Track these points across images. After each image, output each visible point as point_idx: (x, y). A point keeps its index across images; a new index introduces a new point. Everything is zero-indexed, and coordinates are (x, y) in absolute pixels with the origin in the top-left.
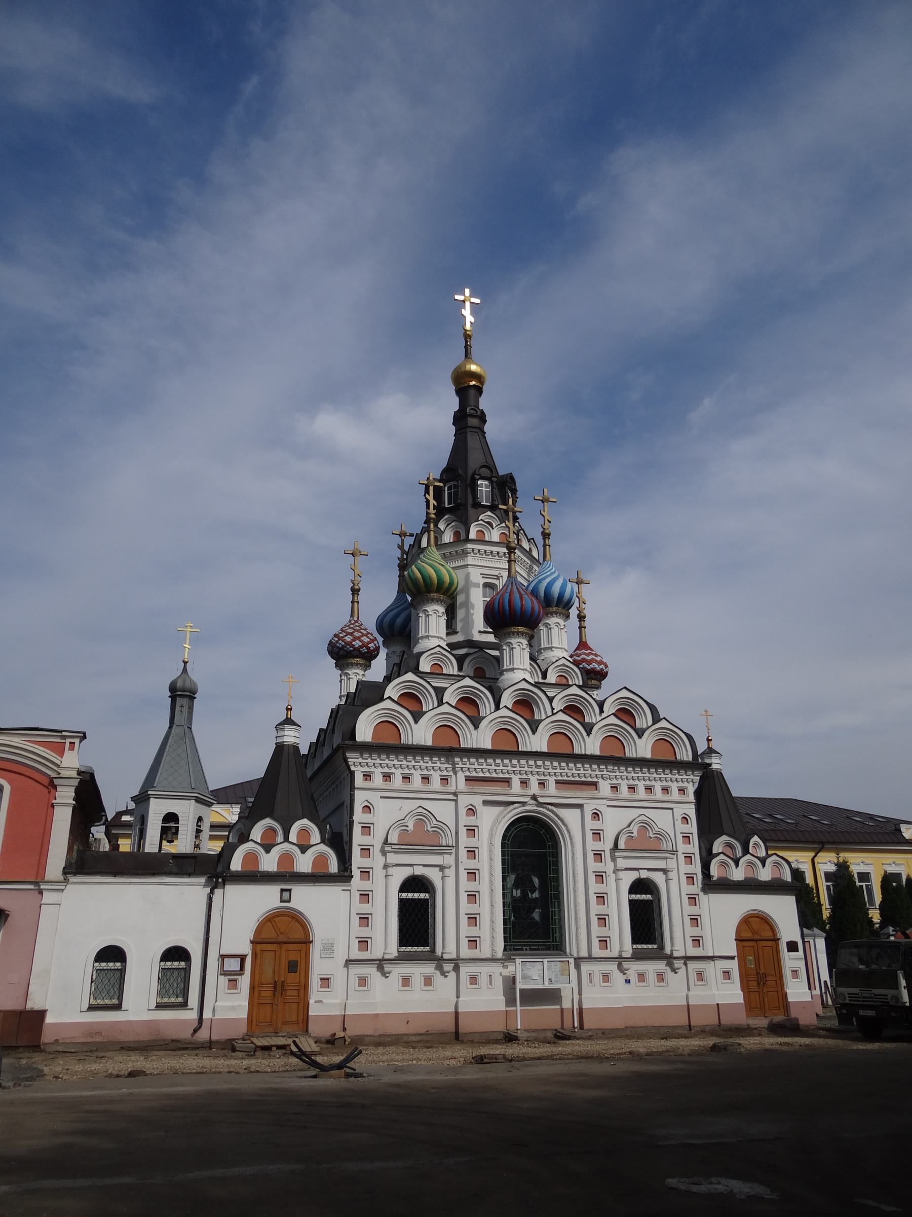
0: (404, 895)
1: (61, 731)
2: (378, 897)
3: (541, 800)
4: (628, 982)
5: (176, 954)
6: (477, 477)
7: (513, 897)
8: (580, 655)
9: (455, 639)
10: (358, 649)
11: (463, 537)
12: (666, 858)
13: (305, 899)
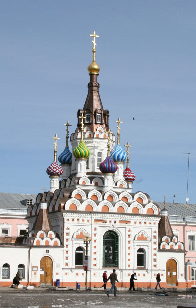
0: (77, 252)
2: (70, 252)
3: (115, 226)
5: (21, 266)
10: (57, 173)
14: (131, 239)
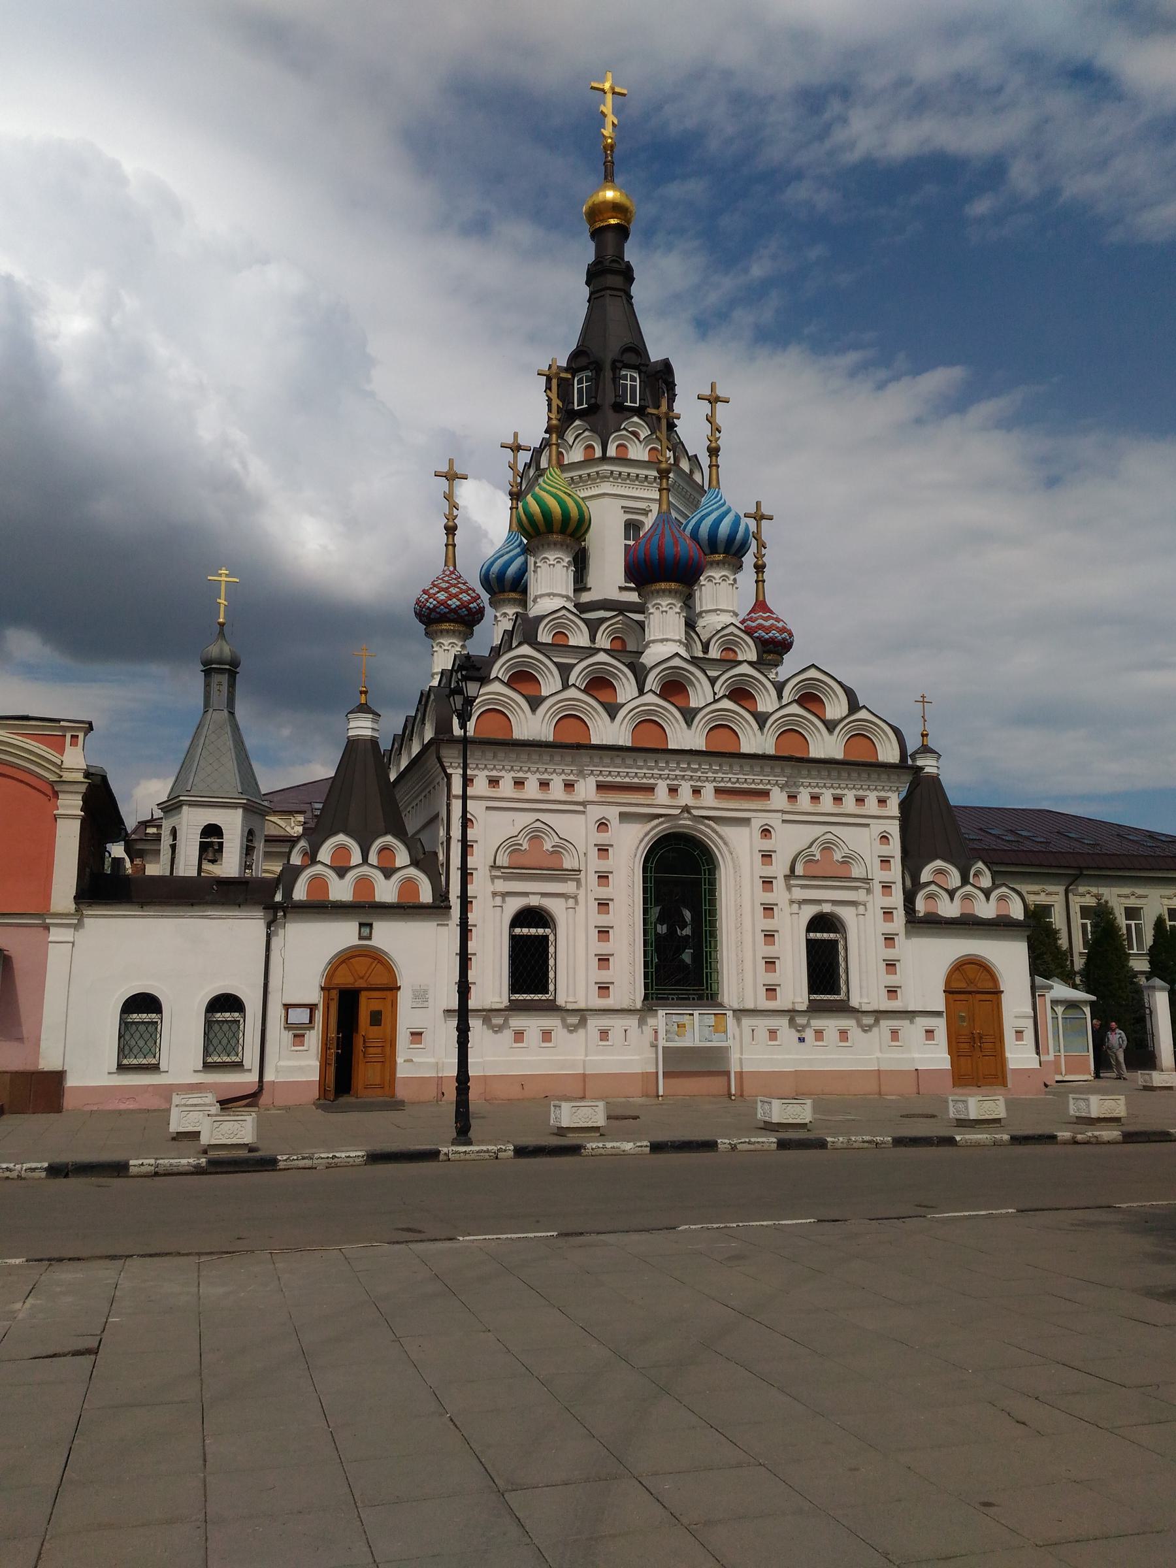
1: (59, 721)
3: (695, 812)
4: (802, 1040)
5: (225, 1004)
6: (619, 365)
7: (657, 934)
8: (757, 619)
9: (586, 597)
10: (454, 611)
11: (598, 453)
12: (857, 888)
13: (389, 936)
14: (779, 868)
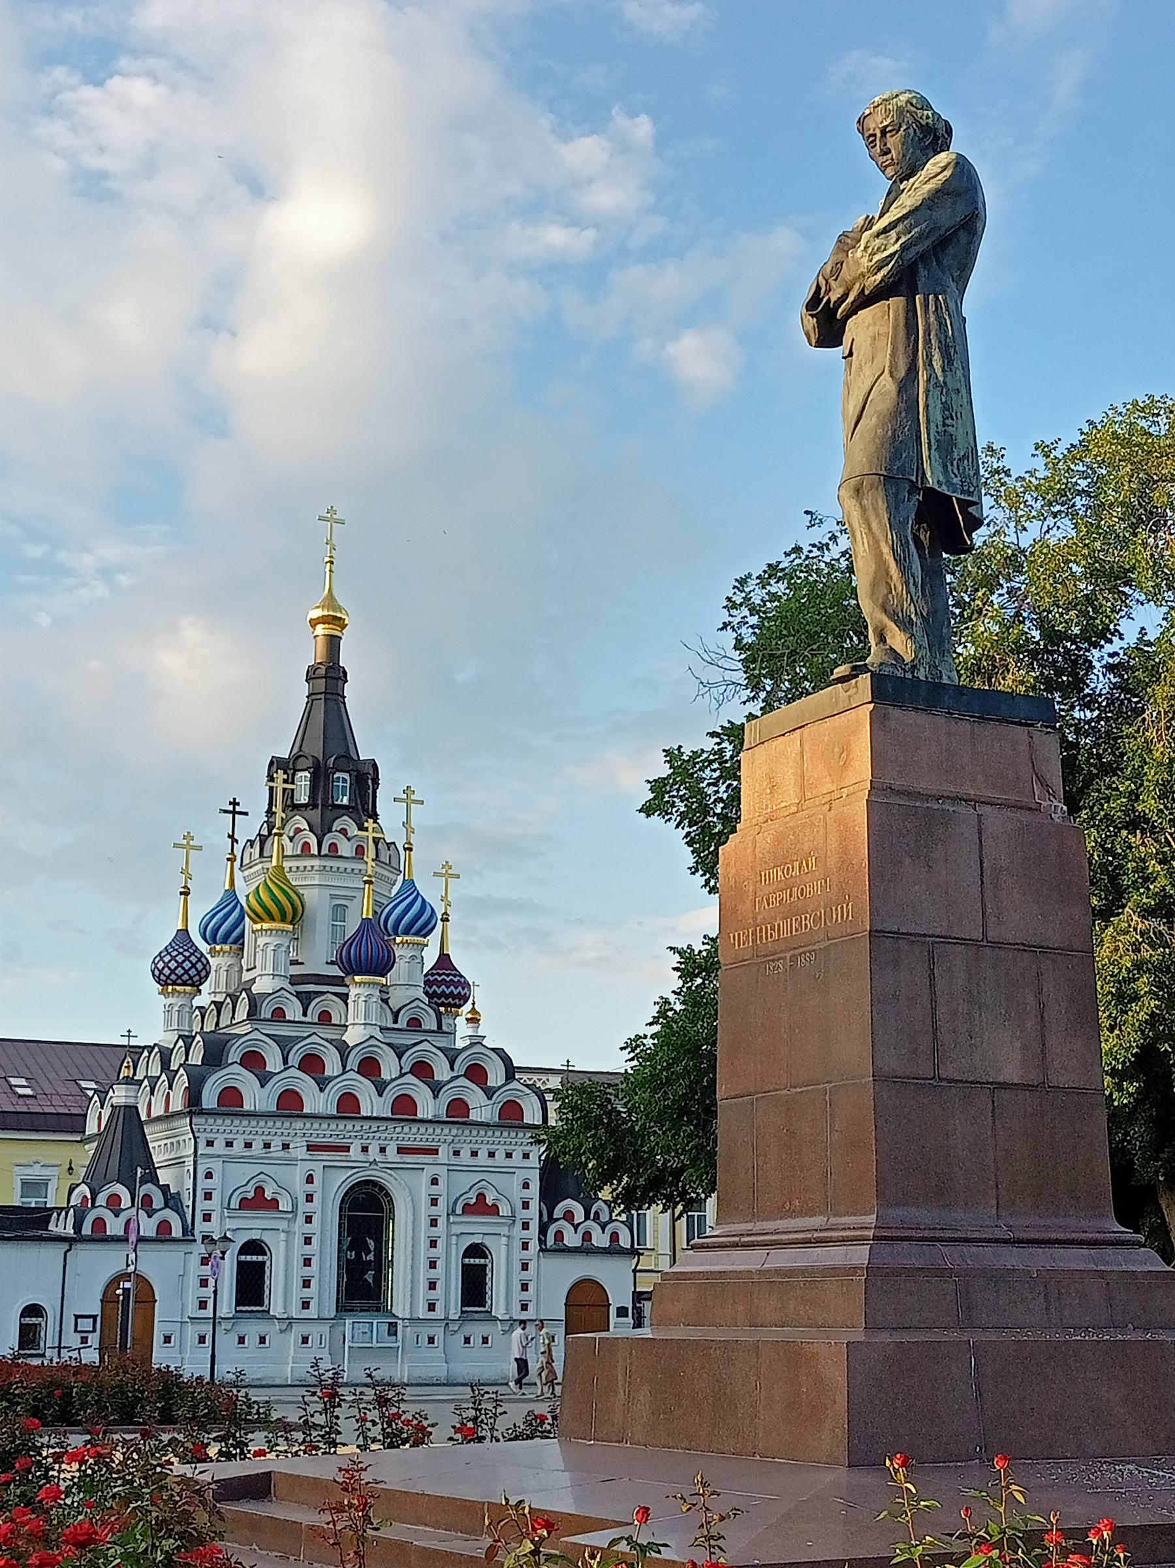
5: (33, 1310)
11: (314, 850)
14: (442, 1208)
